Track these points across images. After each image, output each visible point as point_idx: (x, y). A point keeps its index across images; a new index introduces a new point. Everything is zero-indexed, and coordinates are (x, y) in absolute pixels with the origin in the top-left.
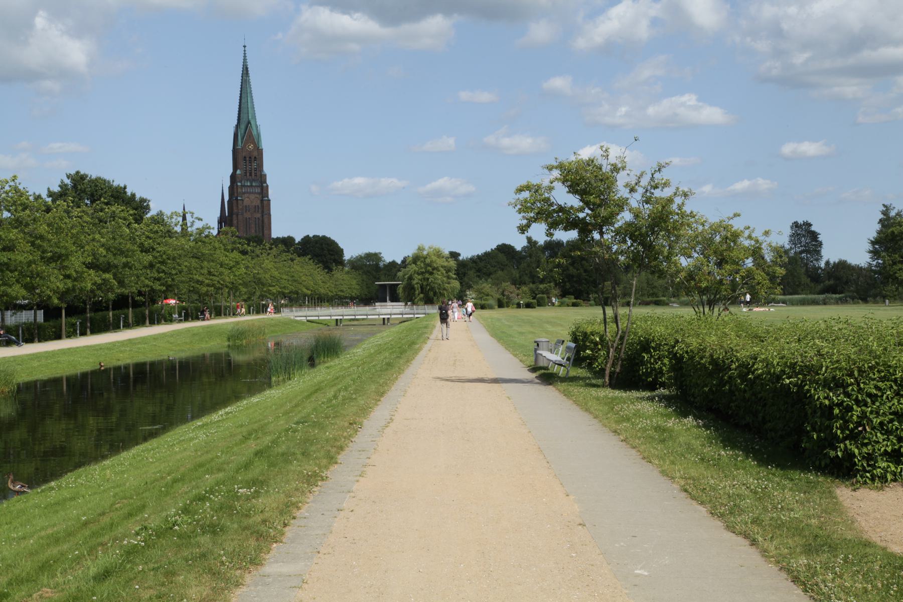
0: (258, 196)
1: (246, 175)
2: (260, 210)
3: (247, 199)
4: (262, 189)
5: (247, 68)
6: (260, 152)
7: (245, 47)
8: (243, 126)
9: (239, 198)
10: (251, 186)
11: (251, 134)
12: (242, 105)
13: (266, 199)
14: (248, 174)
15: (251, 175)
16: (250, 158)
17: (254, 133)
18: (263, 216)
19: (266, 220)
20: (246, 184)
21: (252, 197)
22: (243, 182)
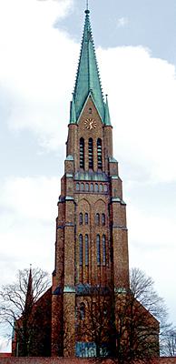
0: (103, 197)
1: (83, 167)
2: (107, 222)
3: (83, 202)
4: (110, 187)
5: (89, 33)
6: (107, 129)
7: (87, 12)
8: (80, 98)
9: (67, 198)
10: (92, 181)
11: (92, 108)
12: (81, 72)
13: (118, 200)
14: (87, 164)
15: (91, 166)
16: (91, 140)
17: (99, 106)
18: (111, 230)
19: (117, 237)
20: (82, 179)
21: (93, 198)
22: (77, 175)
